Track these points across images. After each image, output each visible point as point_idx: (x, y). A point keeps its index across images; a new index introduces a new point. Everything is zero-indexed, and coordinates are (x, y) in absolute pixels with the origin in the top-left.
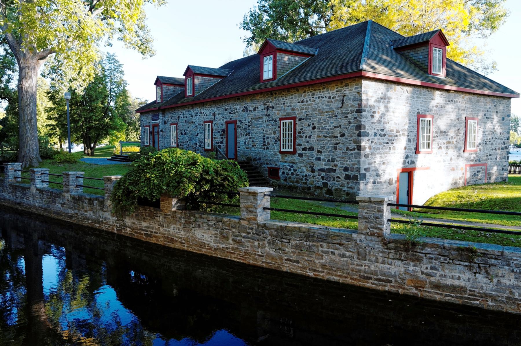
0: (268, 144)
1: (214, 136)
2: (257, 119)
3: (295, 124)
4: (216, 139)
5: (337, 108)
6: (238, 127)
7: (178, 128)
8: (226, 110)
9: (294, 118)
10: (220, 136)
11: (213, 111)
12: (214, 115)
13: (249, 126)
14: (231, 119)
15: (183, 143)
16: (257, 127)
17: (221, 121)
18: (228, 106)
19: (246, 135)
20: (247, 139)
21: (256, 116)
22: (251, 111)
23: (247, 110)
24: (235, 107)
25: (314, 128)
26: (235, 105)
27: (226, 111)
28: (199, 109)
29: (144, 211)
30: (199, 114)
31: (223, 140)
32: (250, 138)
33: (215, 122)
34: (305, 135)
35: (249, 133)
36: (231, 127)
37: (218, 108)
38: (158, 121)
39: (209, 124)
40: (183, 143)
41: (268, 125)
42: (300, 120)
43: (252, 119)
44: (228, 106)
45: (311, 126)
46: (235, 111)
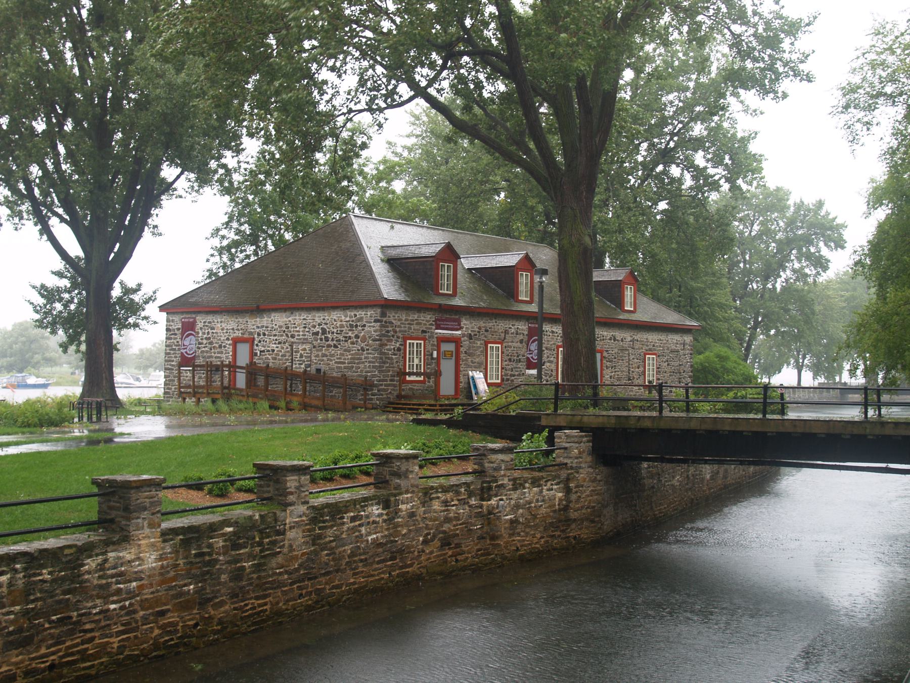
0: (634, 378)
5: (682, 350)
7: (504, 350)
15: (514, 376)
16: (623, 360)
20: (612, 372)
23: (615, 340)
25: (668, 365)
30: (548, 333)
38: (459, 332)
40: (514, 376)
45: (666, 363)
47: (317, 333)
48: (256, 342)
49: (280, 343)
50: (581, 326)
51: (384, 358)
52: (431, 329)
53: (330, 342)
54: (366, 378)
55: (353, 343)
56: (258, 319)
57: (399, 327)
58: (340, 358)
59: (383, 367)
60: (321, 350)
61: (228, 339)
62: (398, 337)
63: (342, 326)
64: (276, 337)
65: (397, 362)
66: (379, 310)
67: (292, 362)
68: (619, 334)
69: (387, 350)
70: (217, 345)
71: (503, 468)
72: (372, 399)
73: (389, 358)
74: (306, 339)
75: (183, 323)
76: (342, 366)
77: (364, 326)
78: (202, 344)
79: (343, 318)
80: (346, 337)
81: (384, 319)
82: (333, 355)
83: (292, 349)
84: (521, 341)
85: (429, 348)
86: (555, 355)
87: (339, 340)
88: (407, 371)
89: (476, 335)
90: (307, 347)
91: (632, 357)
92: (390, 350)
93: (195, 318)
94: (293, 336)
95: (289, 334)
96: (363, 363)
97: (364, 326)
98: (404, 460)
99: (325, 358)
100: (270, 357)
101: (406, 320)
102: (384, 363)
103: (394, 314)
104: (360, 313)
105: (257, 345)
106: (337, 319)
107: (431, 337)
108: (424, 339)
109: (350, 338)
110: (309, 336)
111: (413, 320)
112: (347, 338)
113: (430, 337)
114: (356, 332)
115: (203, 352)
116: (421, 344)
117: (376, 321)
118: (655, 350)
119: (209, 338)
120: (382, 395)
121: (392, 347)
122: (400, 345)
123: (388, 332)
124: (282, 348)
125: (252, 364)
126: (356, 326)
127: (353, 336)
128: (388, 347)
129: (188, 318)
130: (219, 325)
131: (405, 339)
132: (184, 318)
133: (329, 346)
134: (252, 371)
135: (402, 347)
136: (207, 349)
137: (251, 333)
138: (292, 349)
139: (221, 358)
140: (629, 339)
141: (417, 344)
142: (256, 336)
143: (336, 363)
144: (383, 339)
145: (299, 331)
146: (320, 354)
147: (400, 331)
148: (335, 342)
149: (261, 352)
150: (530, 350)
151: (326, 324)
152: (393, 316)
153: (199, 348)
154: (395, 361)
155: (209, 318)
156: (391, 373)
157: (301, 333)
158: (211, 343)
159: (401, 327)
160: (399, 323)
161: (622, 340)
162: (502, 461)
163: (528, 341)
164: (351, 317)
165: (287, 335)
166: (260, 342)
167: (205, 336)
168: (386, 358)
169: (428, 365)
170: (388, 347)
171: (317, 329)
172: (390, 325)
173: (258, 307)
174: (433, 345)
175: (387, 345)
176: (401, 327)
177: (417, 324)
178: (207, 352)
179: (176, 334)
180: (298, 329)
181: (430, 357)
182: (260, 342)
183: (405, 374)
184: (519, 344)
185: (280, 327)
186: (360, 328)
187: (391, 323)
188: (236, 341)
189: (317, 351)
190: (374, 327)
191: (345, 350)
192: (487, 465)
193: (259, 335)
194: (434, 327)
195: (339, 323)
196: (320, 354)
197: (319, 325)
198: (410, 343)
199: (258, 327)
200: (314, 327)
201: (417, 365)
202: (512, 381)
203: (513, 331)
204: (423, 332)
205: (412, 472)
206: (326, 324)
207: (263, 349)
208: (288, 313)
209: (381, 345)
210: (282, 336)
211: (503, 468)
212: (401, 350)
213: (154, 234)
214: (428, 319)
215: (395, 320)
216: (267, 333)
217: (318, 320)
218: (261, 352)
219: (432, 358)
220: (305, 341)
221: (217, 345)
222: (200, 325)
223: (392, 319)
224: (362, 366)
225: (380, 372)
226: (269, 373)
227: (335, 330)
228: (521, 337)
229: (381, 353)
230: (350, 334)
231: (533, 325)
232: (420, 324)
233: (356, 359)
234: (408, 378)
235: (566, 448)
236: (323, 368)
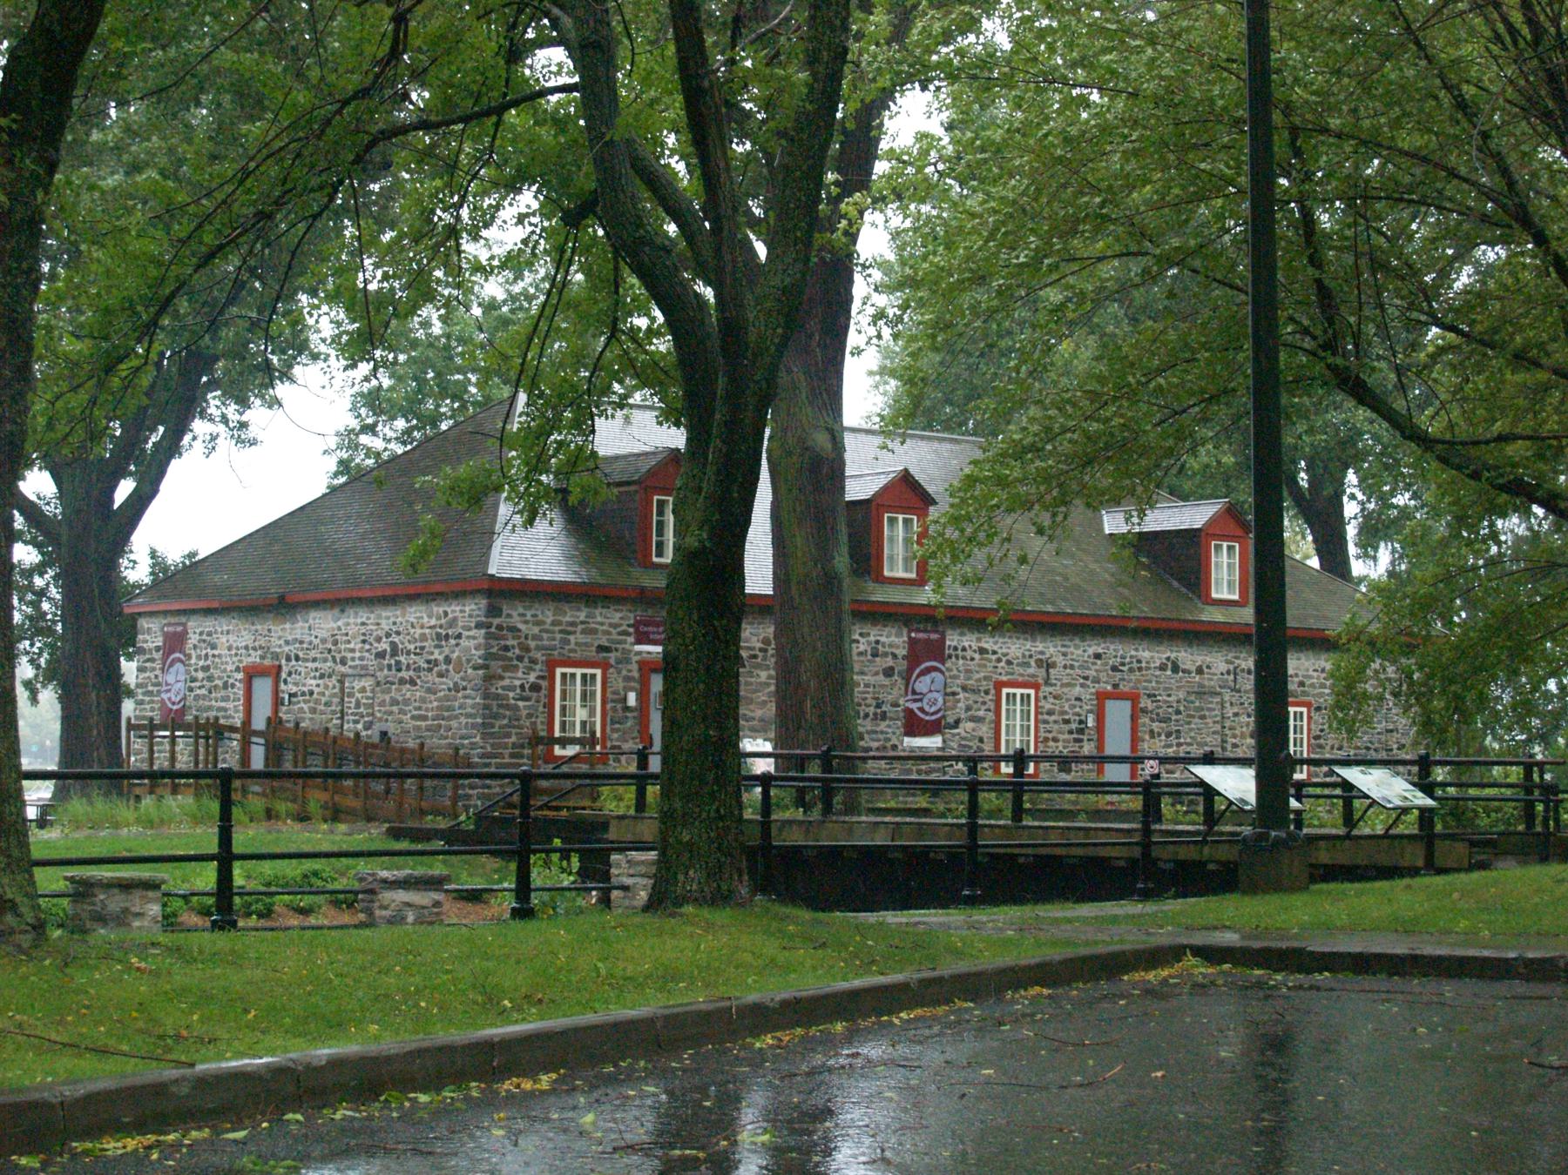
1: (1042, 734)
2: (1201, 693)
3: (1310, 718)
9: (1308, 705)
10: (1071, 732)
11: (1042, 653)
14: (1115, 686)
16: (1203, 717)
19: (1169, 735)
21: (1202, 686)
22: (1189, 672)
28: (974, 637)
30: (969, 654)
32: (1179, 745)
34: (1330, 742)
35: (1178, 731)
36: (1118, 712)
39: (1026, 691)
41: (1236, 715)
42: (1318, 709)
47: (381, 655)
48: (284, 675)
49: (322, 676)
50: (806, 630)
51: (492, 707)
52: (625, 642)
53: (404, 674)
54: (457, 749)
55: (441, 675)
56: (288, 626)
57: (535, 638)
58: (420, 708)
59: (493, 726)
60: (389, 690)
61: (238, 669)
62: (533, 661)
63: (423, 638)
64: (316, 665)
65: (529, 716)
66: (484, 602)
67: (342, 718)
68: (1189, 657)
69: (503, 688)
70: (220, 683)
71: (410, 919)
72: (468, 797)
73: (508, 707)
74: (364, 667)
75: (167, 636)
76: (423, 724)
77: (459, 636)
78: (194, 680)
79: (426, 620)
80: (429, 662)
81: (496, 621)
82: (407, 702)
83: (342, 690)
84: (889, 672)
85: (617, 683)
86: (992, 706)
87: (417, 669)
88: (557, 734)
89: (755, 657)
90: (367, 683)
91: (1230, 712)
92: (511, 688)
93: (184, 625)
94: (343, 662)
95: (338, 657)
96: (456, 717)
97: (459, 636)
98: (116, 891)
99: (395, 709)
100: (305, 707)
101: (554, 623)
102: (496, 716)
103: (521, 610)
104: (454, 609)
105: (285, 682)
106: (417, 619)
107: (628, 661)
108: (605, 666)
109: (436, 663)
110: (371, 662)
111: (573, 624)
112: (433, 663)
113: (619, 662)
114: (446, 651)
115: (197, 698)
116: (593, 676)
117: (479, 626)
118: (1304, 693)
119: (205, 669)
120: (489, 787)
121: (517, 683)
122: (539, 677)
123: (506, 648)
124: (326, 687)
125: (274, 722)
126: (447, 637)
127: (441, 658)
128: (506, 682)
129: (171, 625)
130: (224, 639)
131: (551, 665)
132: (169, 625)
133: (402, 681)
134: (278, 737)
135: (544, 684)
136: (203, 691)
137: (276, 656)
138: (342, 690)
139: (225, 710)
140: (1223, 667)
141: (584, 676)
142: (283, 662)
143: (413, 718)
144: (496, 660)
145: (353, 651)
146: (387, 698)
147: (538, 648)
148: (411, 673)
149: (291, 695)
150: (914, 692)
151: (398, 633)
152: (516, 614)
153: (191, 690)
154: (524, 713)
155: (209, 624)
156: (513, 739)
157: (357, 654)
158: (210, 679)
159: (541, 639)
160: (536, 630)
161: (1200, 671)
162: (408, 904)
163: (910, 670)
164: (439, 618)
165: (334, 658)
166: (290, 674)
167: (201, 663)
168: (500, 706)
169: (613, 722)
170: (506, 682)
171: (384, 646)
172: (510, 635)
173: (282, 598)
174: (628, 679)
175: (502, 678)
176: (541, 639)
177: (584, 631)
178: (204, 697)
179: (152, 660)
180: (352, 646)
181: (619, 706)
182: (290, 674)
183: (554, 741)
184: (881, 677)
185: (324, 641)
186: (453, 642)
187: (513, 629)
188: (251, 674)
189: (383, 692)
190: (474, 638)
191: (429, 691)
192: (378, 913)
193: (288, 659)
194: (631, 639)
195: (419, 631)
196: (387, 698)
197: (388, 635)
198: (564, 675)
199: (287, 643)
200: (379, 640)
203: (862, 648)
204: (601, 649)
205: (140, 915)
206: (398, 633)
207: (294, 689)
208: (336, 611)
209: (489, 679)
210: (325, 660)
211: (410, 919)
212: (541, 690)
213: (240, 441)
214: (615, 621)
215: (526, 622)
216: (301, 654)
217: (385, 625)
218: (291, 695)
219: (627, 708)
220: (363, 673)
221: (220, 683)
222: (193, 639)
223: (516, 621)
224: (454, 724)
225: (484, 736)
226: (306, 741)
227: (412, 647)
228: (889, 662)
229: (486, 696)
230: (437, 655)
231: (921, 636)
232: (593, 632)
233: (445, 712)
234: (558, 751)
235: (625, 888)
236: (391, 728)
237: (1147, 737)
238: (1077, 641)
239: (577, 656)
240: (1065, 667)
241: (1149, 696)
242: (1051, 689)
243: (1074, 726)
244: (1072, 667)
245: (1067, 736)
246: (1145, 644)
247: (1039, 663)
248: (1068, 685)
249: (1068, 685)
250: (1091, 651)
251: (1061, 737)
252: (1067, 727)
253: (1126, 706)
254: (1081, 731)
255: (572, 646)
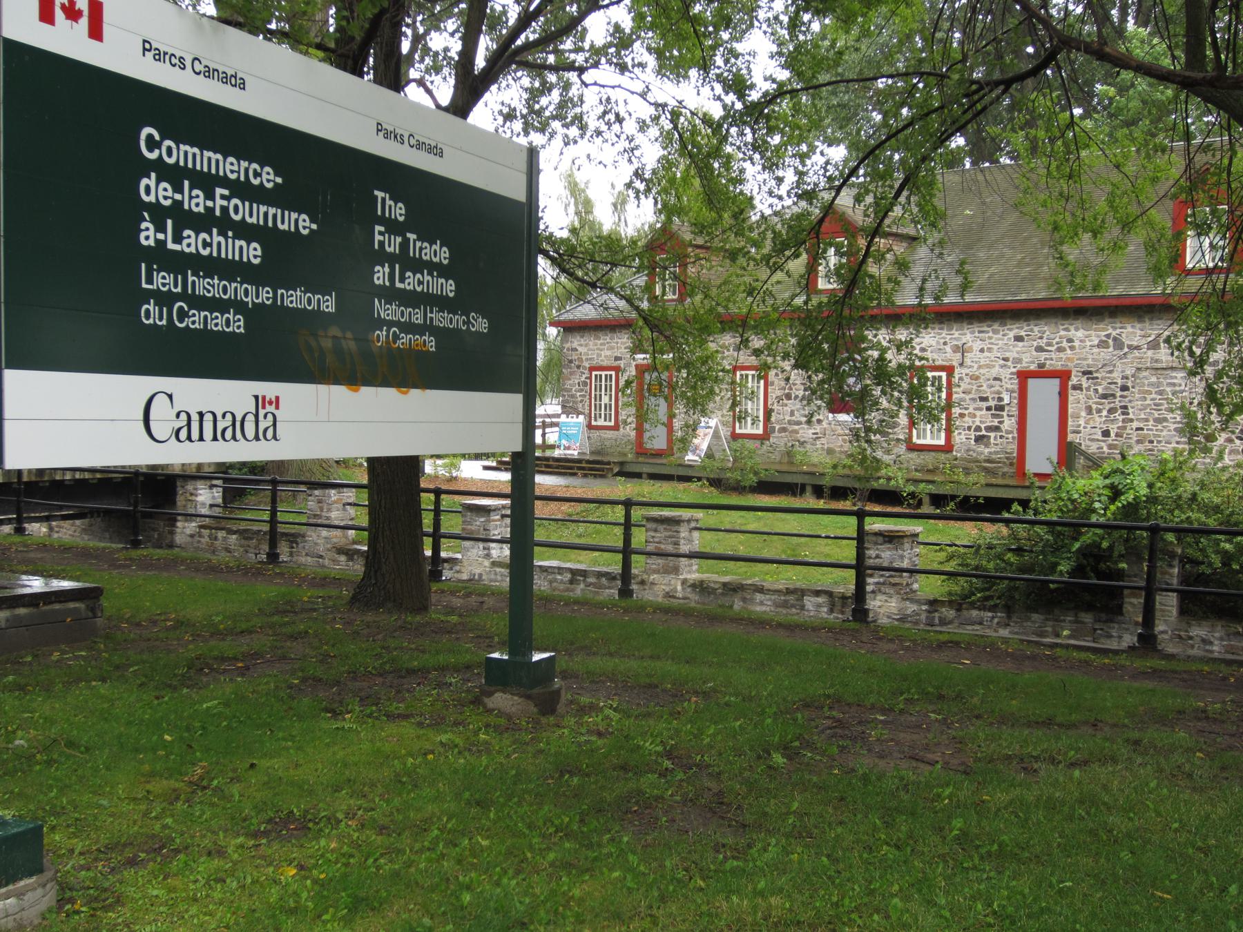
4: (967, 419)
6: (1077, 388)
8: (1019, 339)
10: (989, 409)
12: (962, 350)
13: (1124, 388)
17: (995, 371)
18: (1032, 330)
24: (1063, 333)
26: (1067, 330)
27: (1020, 344)
29: (1051, 623)
31: (1001, 422)
33: (965, 371)
35: (1125, 407)
37: (980, 332)
39: (937, 374)
43: (1139, 369)
44: (1032, 330)
46: (1065, 344)
73: (573, 396)
121: (577, 382)
141: (606, 376)
147: (587, 359)
154: (579, 399)
201: (606, 405)
202: (796, 432)
204: (617, 359)
237: (1083, 414)
238: (996, 326)
239: (605, 364)
240: (982, 351)
241: (1084, 373)
242: (967, 371)
243: (992, 403)
244: (990, 350)
245: (984, 412)
246: (1078, 323)
247: (956, 349)
248: (988, 366)
249: (988, 366)
250: (1011, 334)
251: (978, 413)
252: (985, 405)
253: (1056, 382)
254: (1001, 408)
255: (603, 358)
